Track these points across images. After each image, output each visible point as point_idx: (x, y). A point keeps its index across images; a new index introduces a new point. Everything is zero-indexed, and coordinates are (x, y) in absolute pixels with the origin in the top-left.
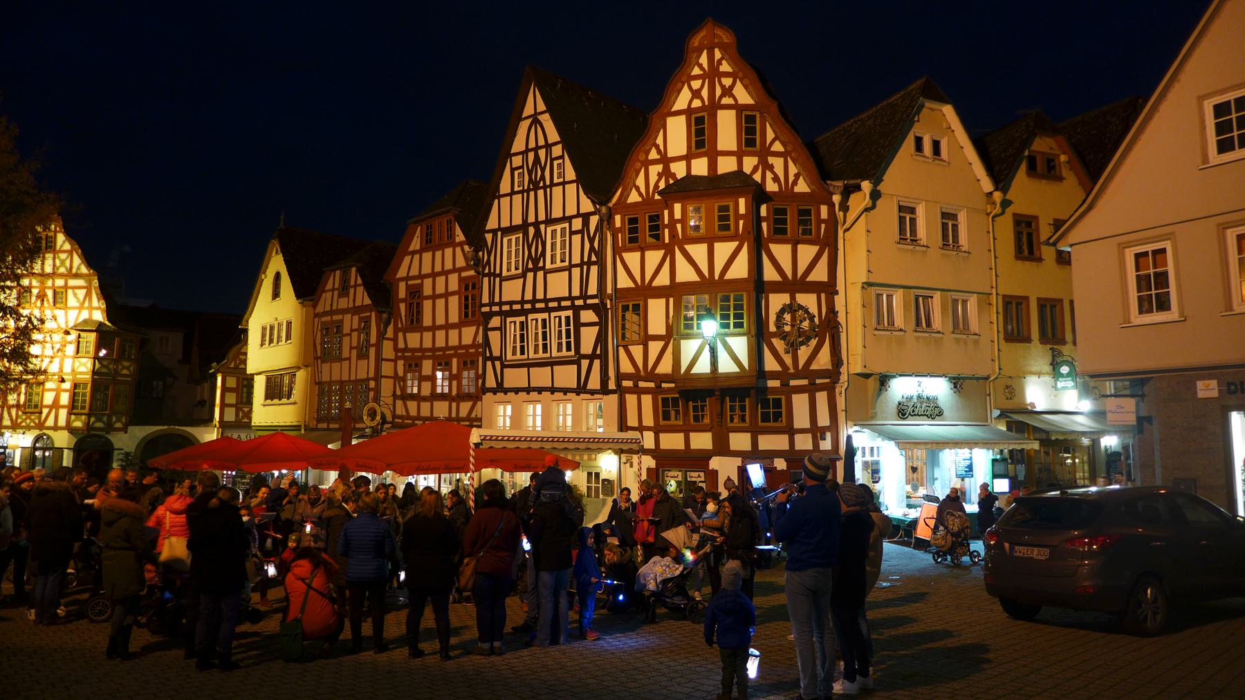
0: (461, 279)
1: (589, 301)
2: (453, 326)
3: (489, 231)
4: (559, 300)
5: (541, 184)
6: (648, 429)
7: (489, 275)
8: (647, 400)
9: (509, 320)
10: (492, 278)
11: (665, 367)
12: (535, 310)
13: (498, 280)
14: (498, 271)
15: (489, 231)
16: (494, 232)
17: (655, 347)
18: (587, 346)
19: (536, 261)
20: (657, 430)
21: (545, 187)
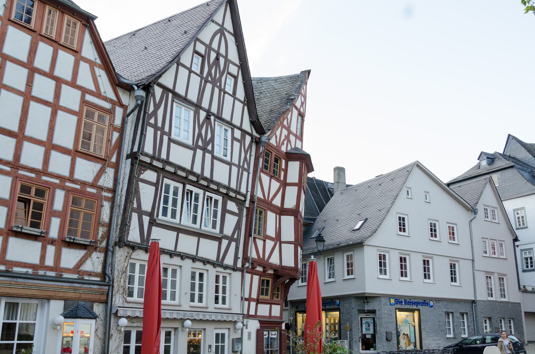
0: (84, 102)
1: (239, 197)
2: (64, 150)
3: (160, 85)
4: (218, 184)
5: (218, 84)
6: (253, 300)
7: (155, 126)
8: (256, 278)
9: (166, 181)
10: (159, 133)
11: (274, 260)
12: (196, 184)
13: (166, 138)
14: (167, 129)
15: (160, 85)
16: (166, 89)
17: (270, 244)
18: (228, 230)
19: (206, 143)
20: (258, 301)
21: (220, 90)
